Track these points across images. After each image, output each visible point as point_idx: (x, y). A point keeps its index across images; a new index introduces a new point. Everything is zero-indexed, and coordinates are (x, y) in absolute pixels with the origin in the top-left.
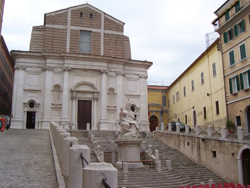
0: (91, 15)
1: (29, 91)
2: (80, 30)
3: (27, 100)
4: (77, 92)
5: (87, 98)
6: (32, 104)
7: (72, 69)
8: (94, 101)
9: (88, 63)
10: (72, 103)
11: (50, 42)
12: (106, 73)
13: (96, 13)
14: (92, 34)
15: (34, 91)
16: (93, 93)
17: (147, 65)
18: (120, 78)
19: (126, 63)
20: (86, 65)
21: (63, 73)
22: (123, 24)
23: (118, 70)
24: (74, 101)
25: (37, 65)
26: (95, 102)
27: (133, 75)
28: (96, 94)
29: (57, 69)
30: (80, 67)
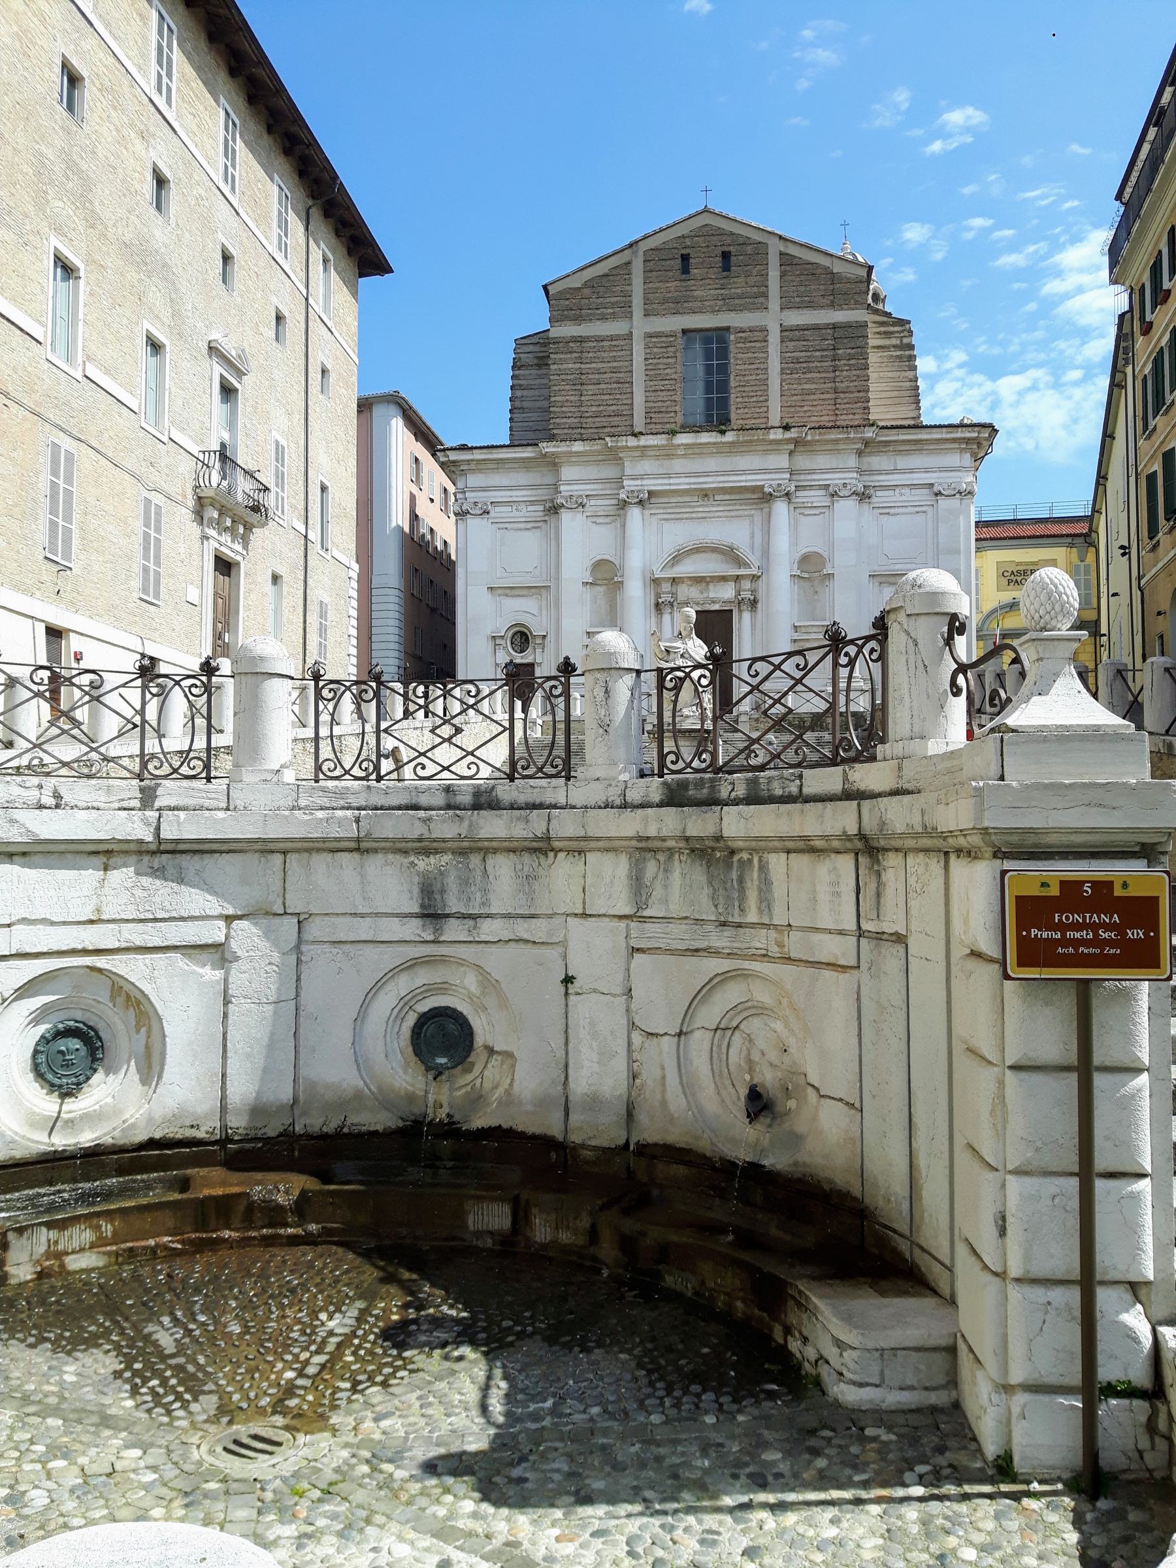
0: (726, 256)
1: (508, 591)
2: (684, 332)
3: (502, 626)
4: (674, 580)
5: (713, 602)
6: (522, 638)
7: (650, 493)
8: (740, 611)
9: (711, 464)
10: (660, 623)
11: (572, 398)
13: (746, 242)
14: (732, 337)
15: (525, 592)
16: (737, 578)
17: (968, 441)
18: (847, 507)
19: (867, 443)
20: (706, 474)
21: (621, 512)
22: (864, 273)
23: (835, 479)
24: (666, 618)
25: (528, 493)
26: (746, 616)
27: (906, 491)
28: (746, 585)
29: (599, 502)
30: (682, 483)
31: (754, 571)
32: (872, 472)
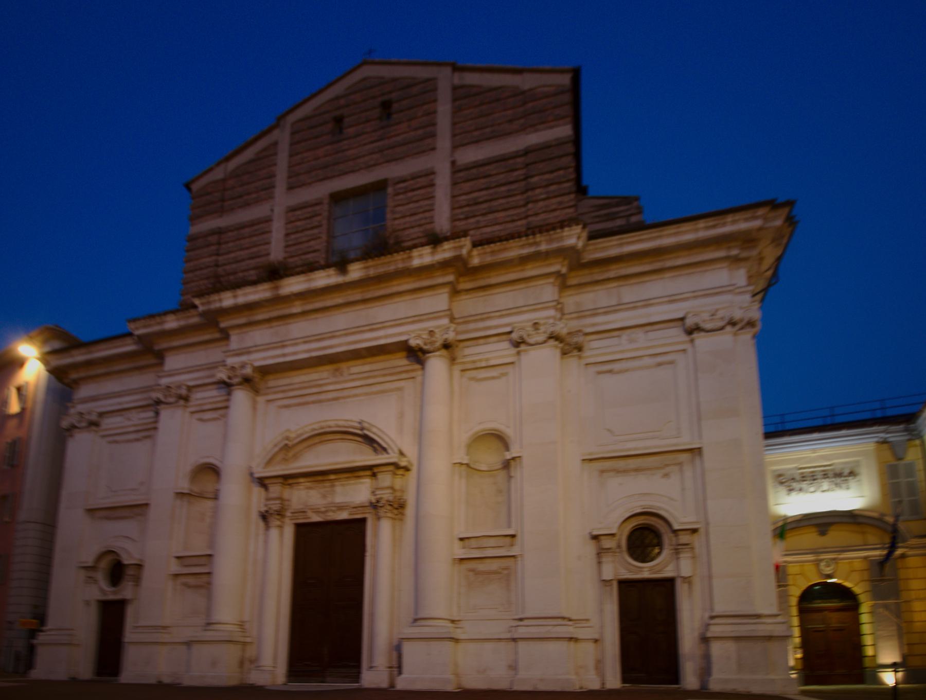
12: (447, 346)
23: (523, 320)
30: (300, 352)
31: (392, 457)
32: (581, 314)
